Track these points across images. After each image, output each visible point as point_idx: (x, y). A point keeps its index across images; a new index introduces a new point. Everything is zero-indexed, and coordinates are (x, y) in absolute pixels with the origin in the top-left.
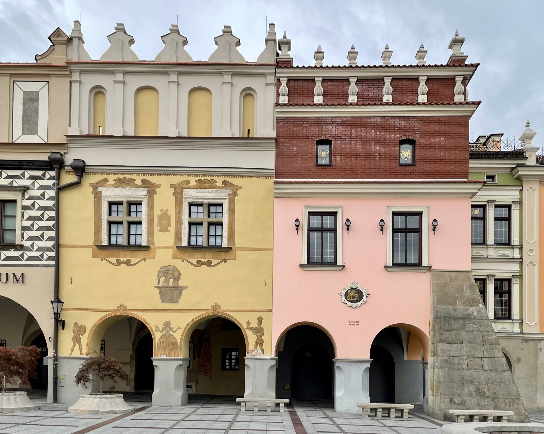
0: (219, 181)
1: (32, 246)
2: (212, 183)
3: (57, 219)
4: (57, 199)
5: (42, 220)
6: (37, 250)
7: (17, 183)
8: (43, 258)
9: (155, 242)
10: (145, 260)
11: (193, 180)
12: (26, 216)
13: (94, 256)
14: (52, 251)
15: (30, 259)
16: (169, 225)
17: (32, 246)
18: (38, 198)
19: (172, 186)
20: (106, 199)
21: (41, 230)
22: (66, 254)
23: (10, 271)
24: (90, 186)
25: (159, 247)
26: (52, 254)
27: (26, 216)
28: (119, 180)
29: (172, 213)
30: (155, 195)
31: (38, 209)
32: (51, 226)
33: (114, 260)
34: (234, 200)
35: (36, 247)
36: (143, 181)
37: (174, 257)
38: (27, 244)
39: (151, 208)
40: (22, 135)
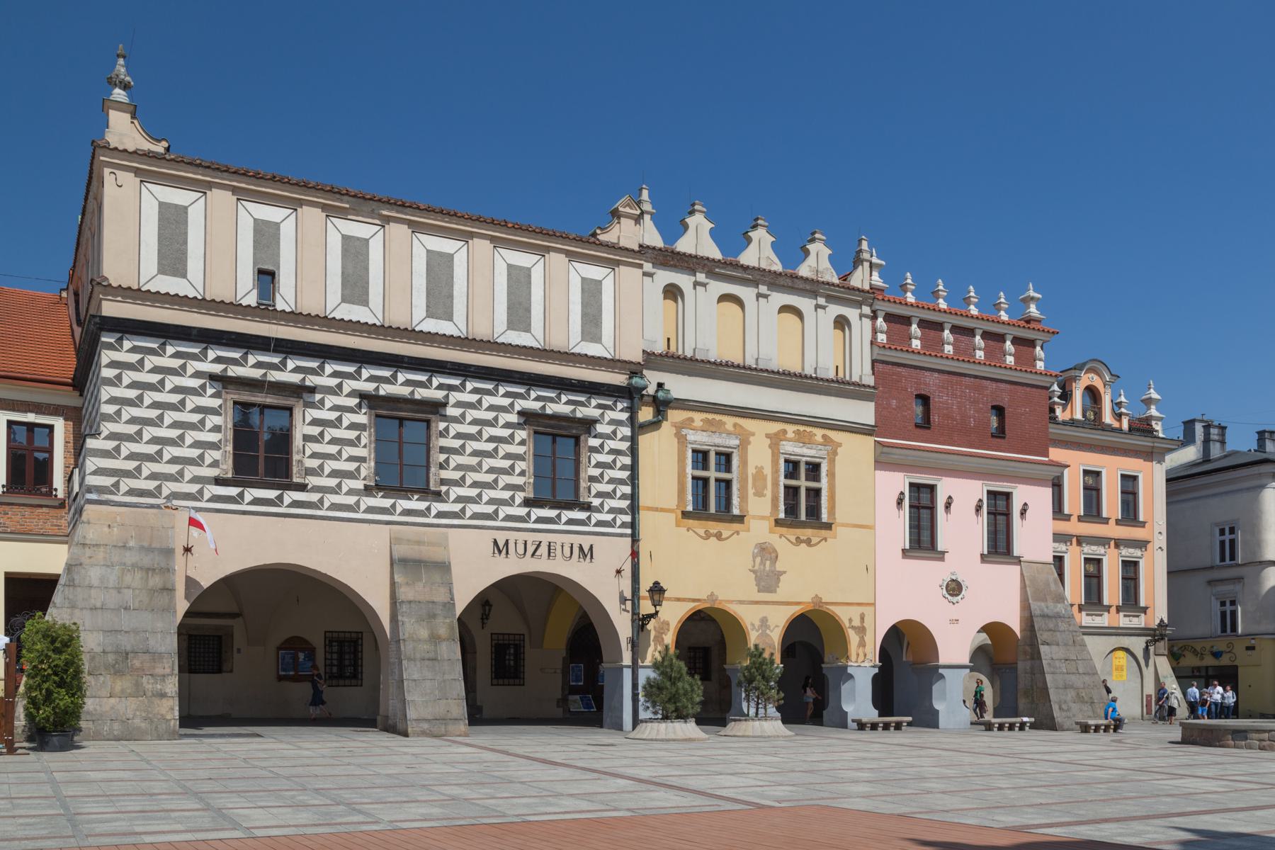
0: (819, 433)
1: (602, 504)
2: (811, 436)
3: (634, 468)
4: (633, 440)
5: (613, 469)
6: (608, 512)
7: (582, 412)
8: (615, 523)
9: (749, 509)
10: (738, 533)
11: (791, 429)
12: (593, 462)
13: (678, 525)
14: (627, 514)
15: (599, 523)
16: (765, 487)
17: (602, 504)
18: (608, 437)
19: (768, 436)
20: (690, 446)
21: (612, 484)
22: (647, 520)
23: (577, 540)
24: (672, 426)
25: (754, 517)
26: (628, 518)
27: (593, 462)
28: (706, 421)
29: (768, 471)
30: (750, 447)
31: (608, 453)
32: (625, 477)
33: (701, 532)
34: (834, 460)
35: (606, 508)
36: (735, 425)
37: (771, 532)
38: (596, 502)
39: (744, 463)
40: (582, 340)
